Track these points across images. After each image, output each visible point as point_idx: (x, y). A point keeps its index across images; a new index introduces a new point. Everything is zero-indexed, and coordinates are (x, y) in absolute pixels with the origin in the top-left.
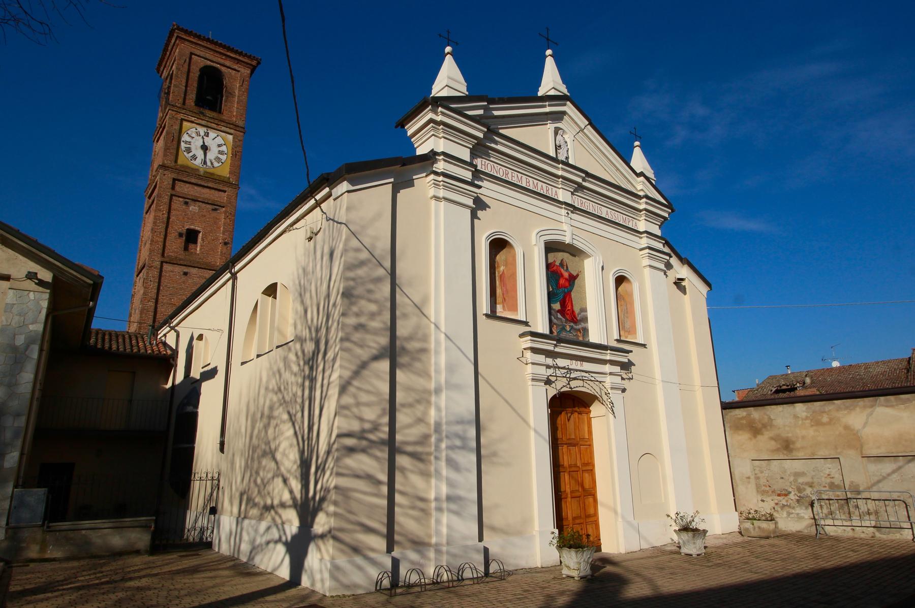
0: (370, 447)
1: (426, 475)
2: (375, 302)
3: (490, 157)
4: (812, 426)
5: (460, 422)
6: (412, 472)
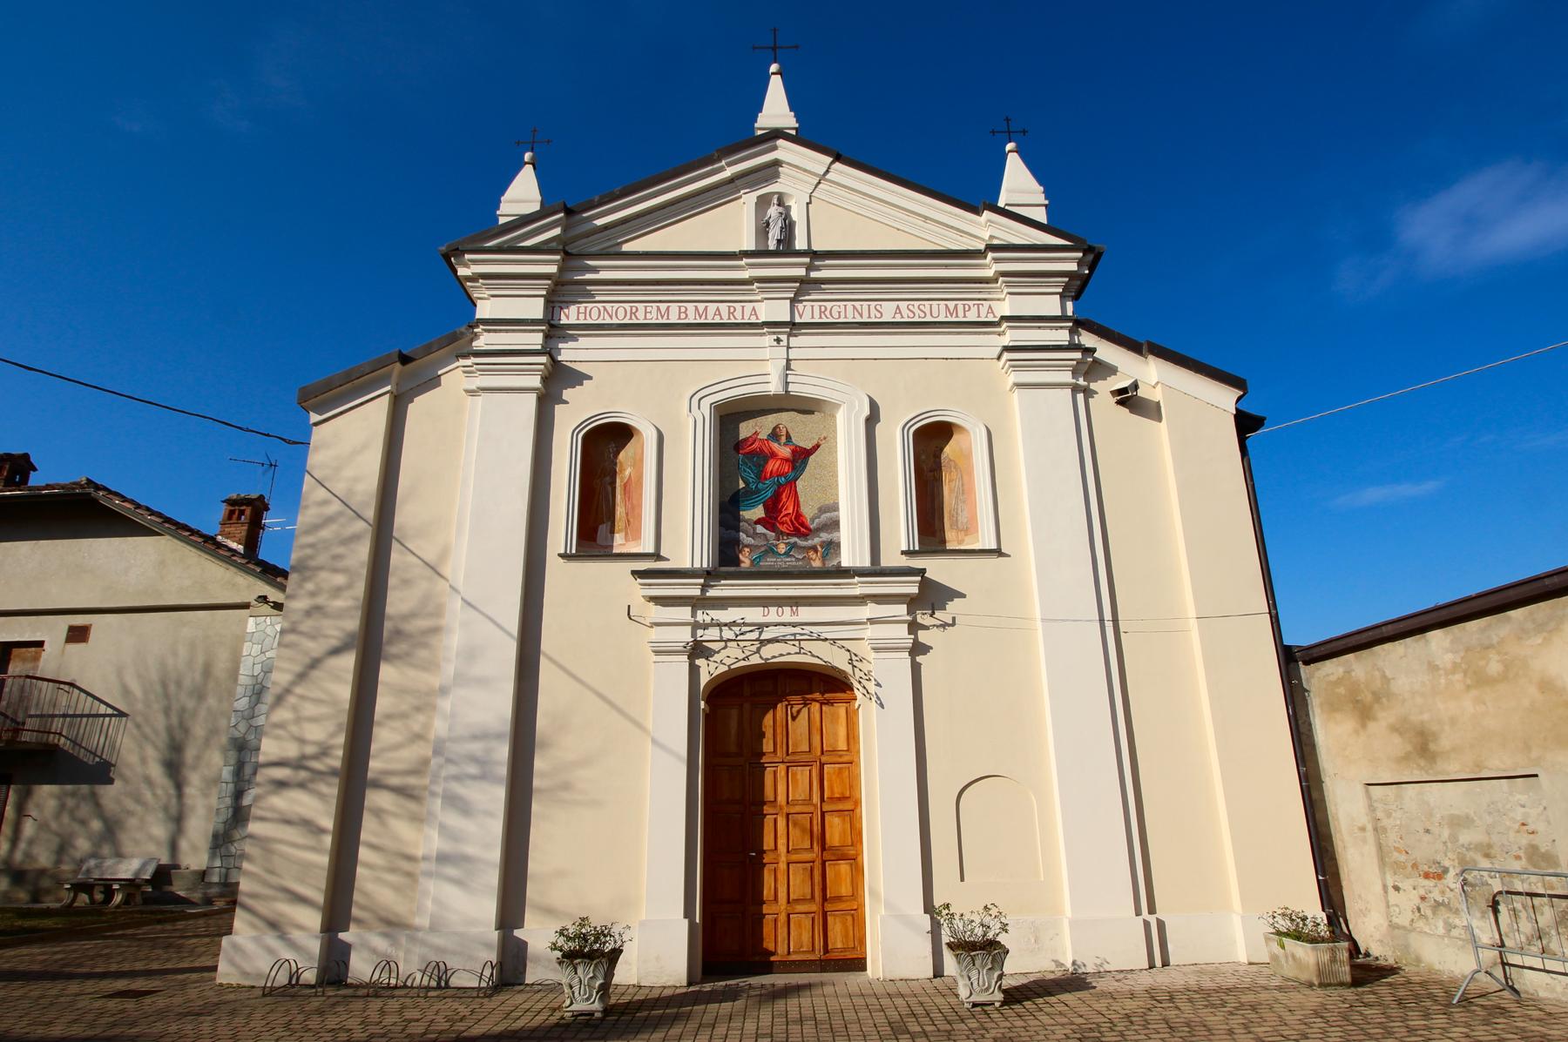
0: (312, 781)
1: (417, 819)
2: (344, 571)
3: (593, 296)
4: (1468, 687)
5: (482, 736)
6: (395, 815)
